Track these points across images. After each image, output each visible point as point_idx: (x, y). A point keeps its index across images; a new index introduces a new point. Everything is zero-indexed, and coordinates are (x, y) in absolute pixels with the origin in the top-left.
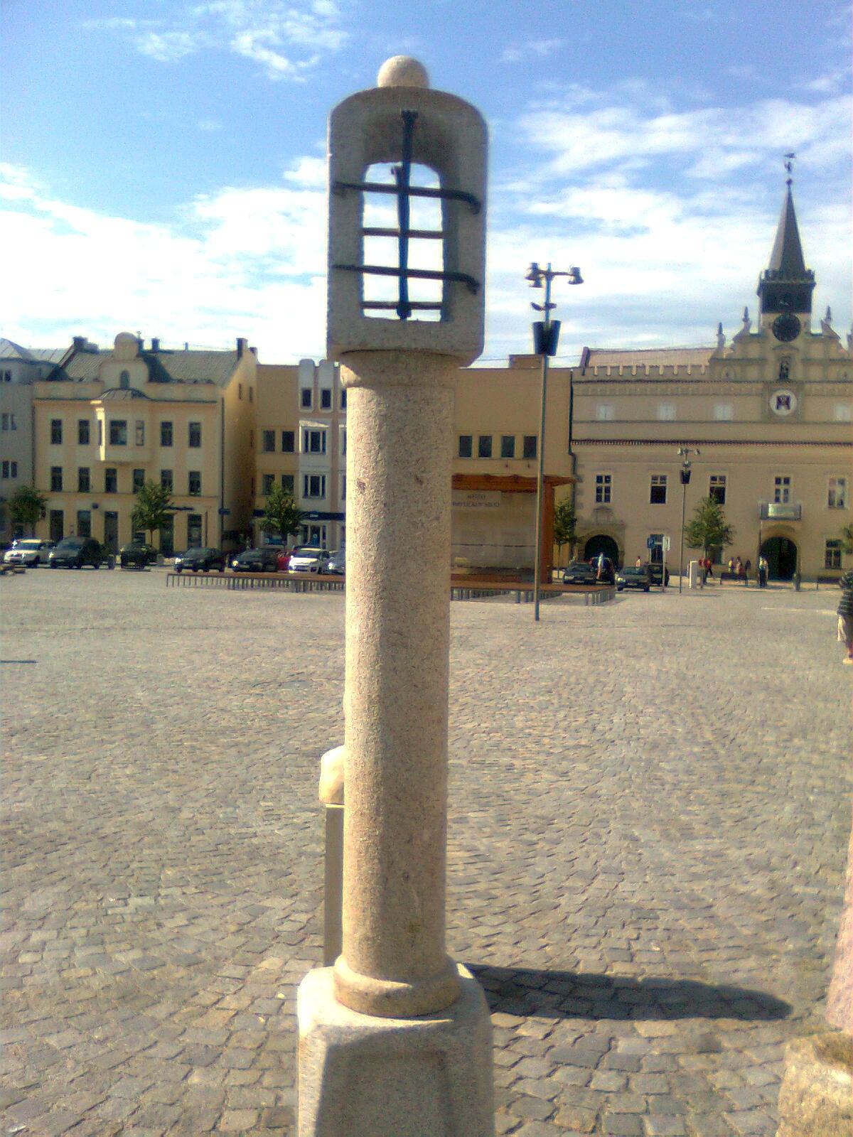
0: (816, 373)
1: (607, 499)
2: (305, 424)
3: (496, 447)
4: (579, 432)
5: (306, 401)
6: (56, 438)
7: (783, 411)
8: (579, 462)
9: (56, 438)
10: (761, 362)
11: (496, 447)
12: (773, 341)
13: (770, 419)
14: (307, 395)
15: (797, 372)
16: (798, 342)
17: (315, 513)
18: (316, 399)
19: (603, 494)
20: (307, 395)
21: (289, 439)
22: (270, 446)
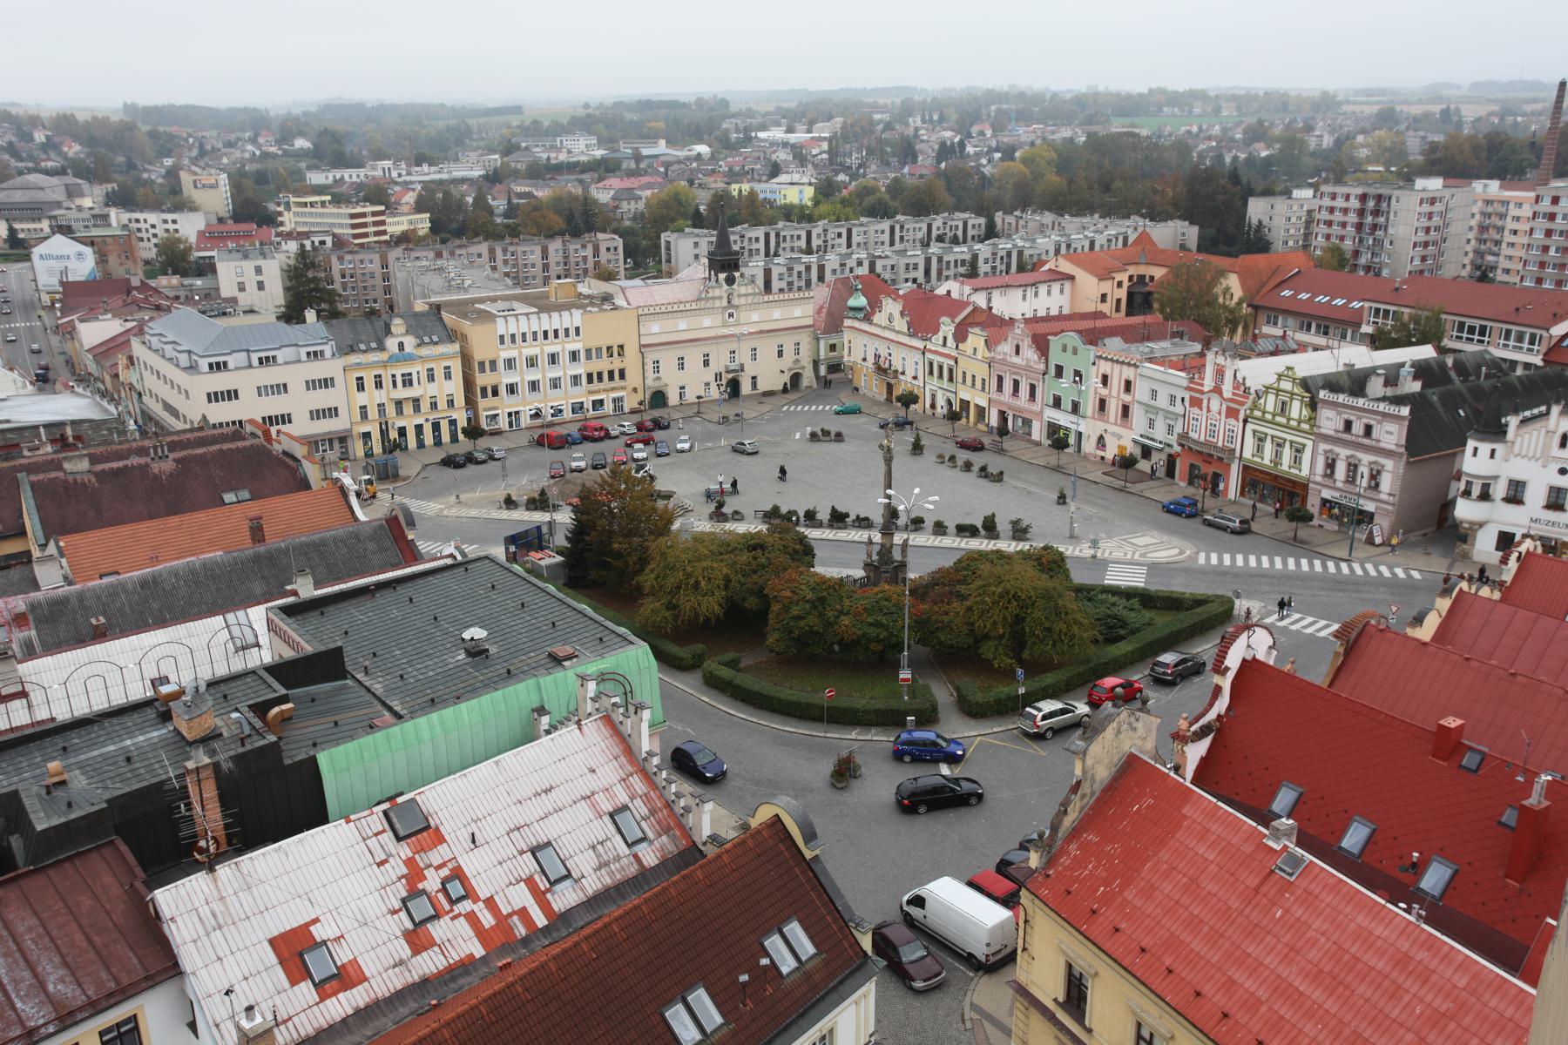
0: (743, 301)
2: (505, 354)
6: (361, 387)
9: (361, 387)
10: (720, 298)
12: (725, 287)
14: (502, 337)
15: (736, 301)
16: (735, 286)
18: (507, 339)
19: (657, 369)
20: (502, 337)
21: (493, 363)
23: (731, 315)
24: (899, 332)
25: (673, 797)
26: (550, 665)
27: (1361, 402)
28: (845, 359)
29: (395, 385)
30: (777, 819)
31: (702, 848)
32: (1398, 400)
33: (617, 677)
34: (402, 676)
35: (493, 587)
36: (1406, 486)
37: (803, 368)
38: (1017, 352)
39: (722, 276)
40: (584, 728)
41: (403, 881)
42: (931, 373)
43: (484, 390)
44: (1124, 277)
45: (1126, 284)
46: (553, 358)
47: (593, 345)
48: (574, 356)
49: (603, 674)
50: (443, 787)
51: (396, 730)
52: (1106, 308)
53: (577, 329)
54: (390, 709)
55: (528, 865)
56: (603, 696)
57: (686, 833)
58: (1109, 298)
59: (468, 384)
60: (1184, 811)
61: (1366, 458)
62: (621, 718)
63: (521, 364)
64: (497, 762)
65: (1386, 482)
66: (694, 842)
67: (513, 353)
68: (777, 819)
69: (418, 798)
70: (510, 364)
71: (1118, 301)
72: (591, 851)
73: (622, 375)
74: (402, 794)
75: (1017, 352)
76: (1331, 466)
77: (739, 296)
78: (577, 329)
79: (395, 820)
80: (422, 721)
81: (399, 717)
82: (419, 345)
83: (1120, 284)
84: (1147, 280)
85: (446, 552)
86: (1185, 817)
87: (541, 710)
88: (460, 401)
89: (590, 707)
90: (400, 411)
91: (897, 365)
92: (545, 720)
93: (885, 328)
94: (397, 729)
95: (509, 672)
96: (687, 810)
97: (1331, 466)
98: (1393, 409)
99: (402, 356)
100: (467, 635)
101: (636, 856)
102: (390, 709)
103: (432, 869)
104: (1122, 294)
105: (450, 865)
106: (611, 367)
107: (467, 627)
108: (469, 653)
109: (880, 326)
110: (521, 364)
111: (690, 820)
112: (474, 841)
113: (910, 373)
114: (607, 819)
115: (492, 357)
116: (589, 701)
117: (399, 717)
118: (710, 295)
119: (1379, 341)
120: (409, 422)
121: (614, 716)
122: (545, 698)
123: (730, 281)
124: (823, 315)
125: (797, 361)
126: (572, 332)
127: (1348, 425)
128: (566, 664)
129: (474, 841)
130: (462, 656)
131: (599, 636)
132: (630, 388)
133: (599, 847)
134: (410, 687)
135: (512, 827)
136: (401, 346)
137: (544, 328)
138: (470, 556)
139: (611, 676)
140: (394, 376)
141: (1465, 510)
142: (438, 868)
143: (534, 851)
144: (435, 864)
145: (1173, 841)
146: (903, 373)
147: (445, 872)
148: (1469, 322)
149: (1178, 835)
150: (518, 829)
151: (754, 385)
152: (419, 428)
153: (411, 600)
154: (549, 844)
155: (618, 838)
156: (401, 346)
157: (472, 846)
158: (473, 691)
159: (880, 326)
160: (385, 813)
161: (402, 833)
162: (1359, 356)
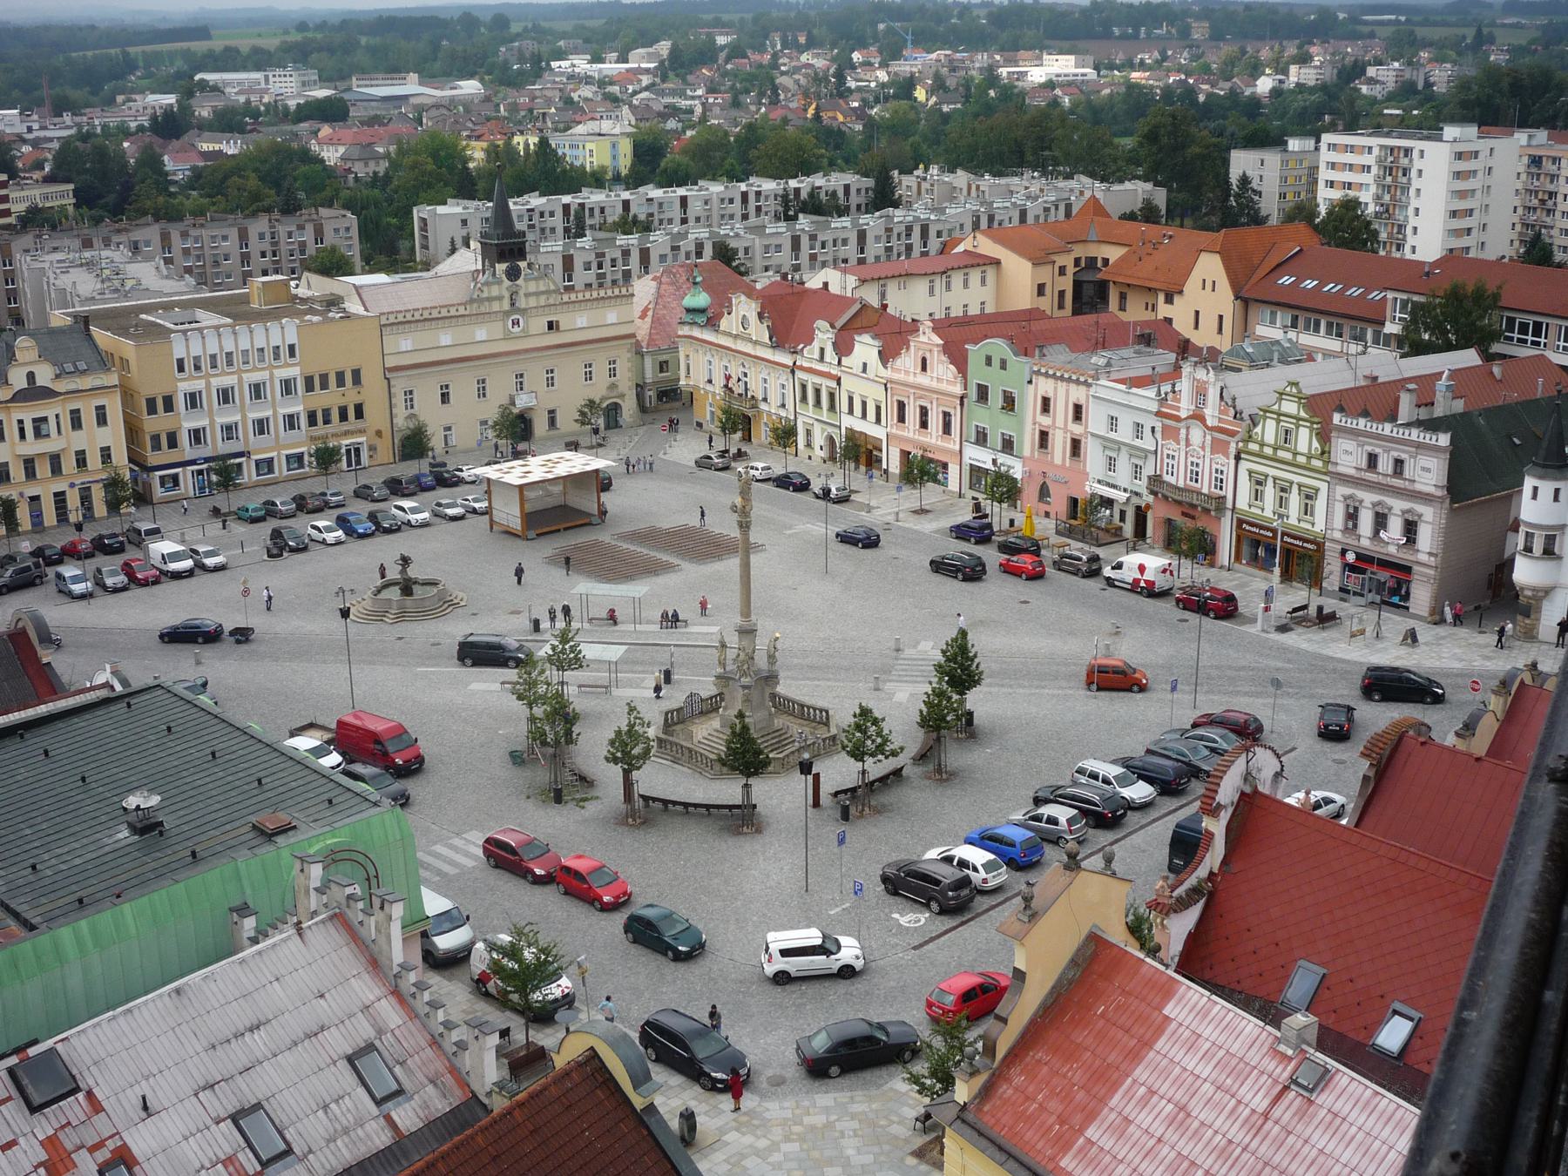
0: (532, 302)
1: (412, 407)
2: (185, 386)
3: (332, 380)
4: (390, 362)
5: (181, 369)
7: (516, 329)
8: (392, 383)
10: (500, 298)
11: (332, 380)
12: (507, 283)
13: (508, 337)
15: (522, 303)
16: (520, 282)
17: (200, 459)
19: (410, 403)
21: (169, 404)
22: (152, 409)
23: (516, 323)
24: (756, 343)
25: (441, 1029)
26: (255, 842)
27: (1387, 428)
28: (682, 382)
29: (22, 436)
30: (593, 1055)
31: (486, 1101)
32: (1432, 425)
33: (354, 856)
34: (34, 867)
35: (169, 729)
36: (1450, 539)
37: (622, 396)
38: (924, 368)
39: (501, 267)
40: (308, 934)
41: (42, 1171)
42: (804, 398)
43: (156, 439)
44: (1067, 260)
45: (1071, 270)
46: (257, 391)
47: (315, 370)
48: (288, 387)
49: (333, 852)
50: (98, 1030)
51: (27, 947)
52: (1046, 304)
53: (292, 348)
54: (16, 915)
55: (226, 1138)
56: (333, 886)
57: (463, 1083)
58: (1048, 290)
59: (133, 432)
60: (1166, 1011)
61: (1398, 505)
62: (361, 917)
63: (210, 400)
64: (178, 991)
65: (1426, 538)
66: (475, 1096)
67: (197, 385)
68: (593, 1055)
69: (59, 1047)
70: (193, 400)
71: (1062, 294)
72: (320, 1113)
73: (359, 413)
74: (35, 1042)
75: (924, 368)
76: (1352, 516)
77: (527, 295)
78: (292, 348)
79: (25, 1081)
80: (65, 933)
81: (32, 928)
82: (57, 376)
83: (1062, 271)
84: (1099, 264)
85: (100, 679)
86: (1167, 1018)
87: (243, 910)
88: (120, 457)
89: (314, 901)
90: (30, 472)
91: (756, 389)
92: (249, 924)
93: (736, 337)
94: (27, 946)
95: (194, 854)
96: (461, 1046)
97: (1352, 516)
98: (1427, 438)
99: (34, 392)
100: (132, 801)
101: (388, 1118)
102: (16, 915)
103: (84, 1152)
104: (1067, 284)
105: (111, 1144)
106: (342, 402)
107: (131, 791)
108: (134, 829)
109: (729, 334)
110: (210, 400)
111: (467, 1061)
112: (145, 1108)
113: (775, 399)
114: (343, 1065)
115: (167, 391)
116: (313, 894)
117: (32, 928)
118: (485, 295)
119: (1412, 346)
120: (46, 489)
121: (350, 913)
122: (248, 891)
123: (513, 274)
124: (648, 319)
125: (613, 386)
126: (284, 352)
127: (1372, 460)
128: (280, 840)
129: (145, 1108)
130: (124, 833)
131: (326, 796)
132: (371, 432)
133: (333, 1106)
134: (47, 881)
135: (202, 1084)
136: (31, 376)
137: (240, 348)
138: (136, 685)
139: (346, 855)
140: (21, 422)
141: (1525, 572)
142: (93, 1149)
143: (235, 1118)
144: (90, 1143)
145: (1151, 1054)
146: (765, 400)
147: (103, 1155)
148: (1520, 318)
149: (1159, 1045)
150: (212, 1086)
151: (552, 422)
152: (60, 498)
153: (46, 753)
154: (258, 1106)
155: (361, 1091)
156: (31, 376)
157: (144, 1115)
158: (142, 884)
159: (729, 334)
160: (11, 1072)
161: (37, 1100)
162: (1384, 363)
